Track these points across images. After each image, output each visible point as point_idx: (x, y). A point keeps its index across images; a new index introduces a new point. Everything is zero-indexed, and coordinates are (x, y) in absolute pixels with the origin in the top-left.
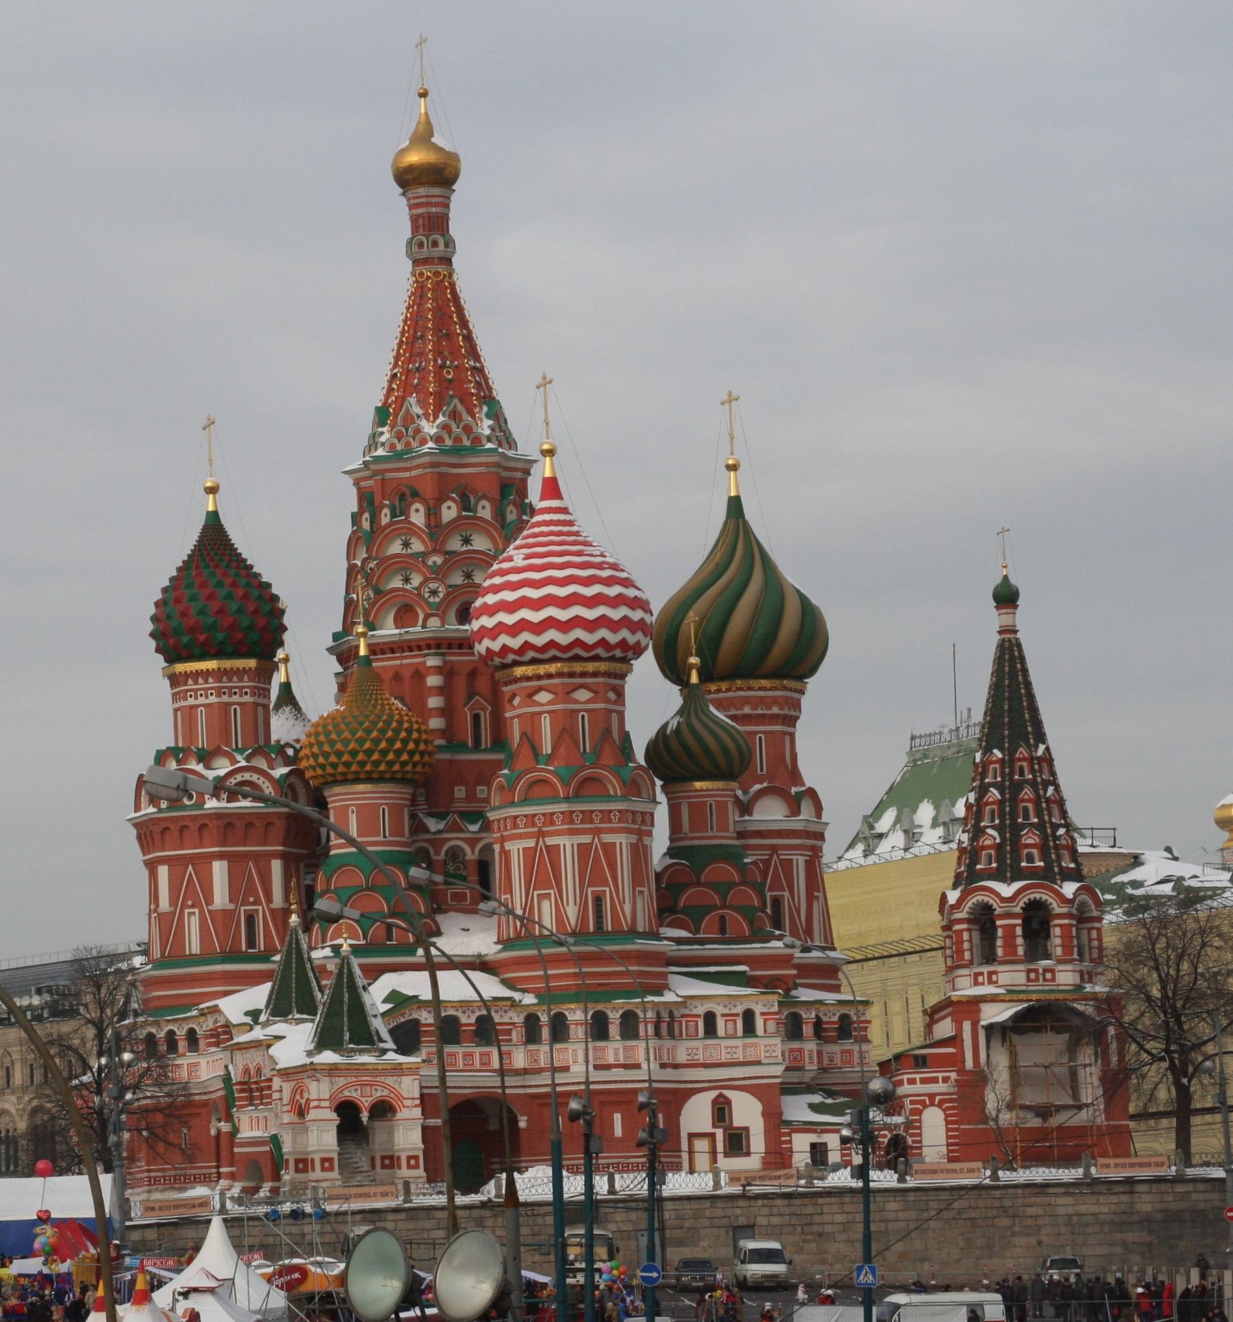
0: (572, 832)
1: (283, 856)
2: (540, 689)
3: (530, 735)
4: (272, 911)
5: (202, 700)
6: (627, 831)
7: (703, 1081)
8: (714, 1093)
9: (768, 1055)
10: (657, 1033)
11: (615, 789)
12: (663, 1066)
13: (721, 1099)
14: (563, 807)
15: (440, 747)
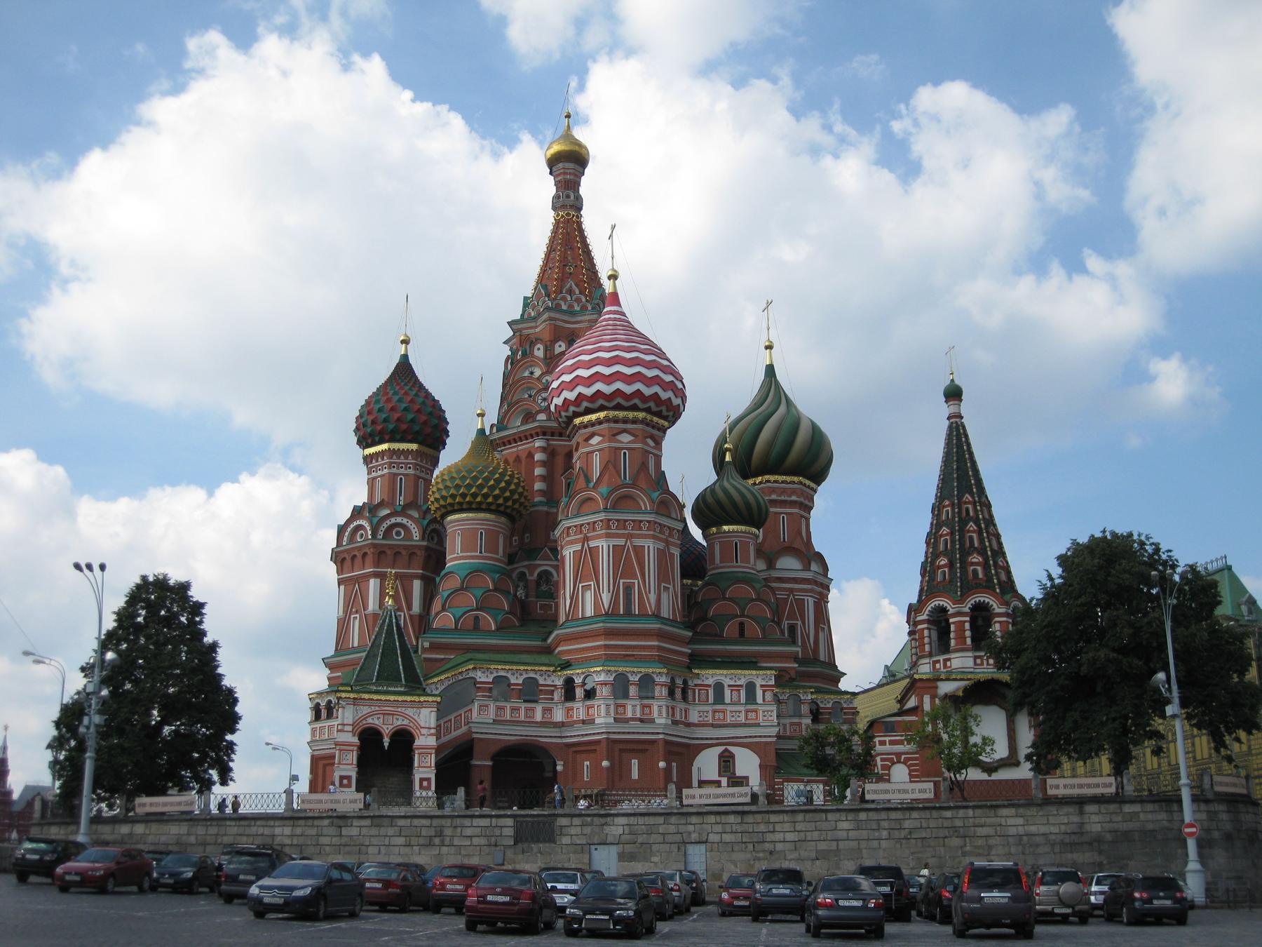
0: (608, 536)
1: (422, 578)
2: (592, 435)
3: (585, 469)
4: (411, 616)
5: (380, 473)
6: (654, 537)
7: (711, 739)
8: (721, 749)
9: (765, 718)
10: (671, 693)
11: (645, 504)
12: (675, 723)
13: (727, 754)
14: (602, 516)
15: (540, 503)
